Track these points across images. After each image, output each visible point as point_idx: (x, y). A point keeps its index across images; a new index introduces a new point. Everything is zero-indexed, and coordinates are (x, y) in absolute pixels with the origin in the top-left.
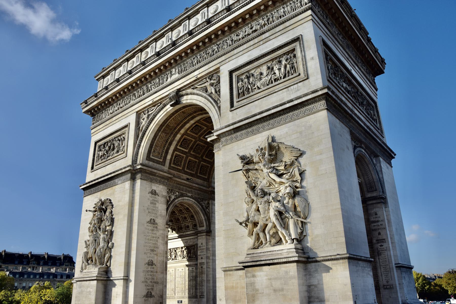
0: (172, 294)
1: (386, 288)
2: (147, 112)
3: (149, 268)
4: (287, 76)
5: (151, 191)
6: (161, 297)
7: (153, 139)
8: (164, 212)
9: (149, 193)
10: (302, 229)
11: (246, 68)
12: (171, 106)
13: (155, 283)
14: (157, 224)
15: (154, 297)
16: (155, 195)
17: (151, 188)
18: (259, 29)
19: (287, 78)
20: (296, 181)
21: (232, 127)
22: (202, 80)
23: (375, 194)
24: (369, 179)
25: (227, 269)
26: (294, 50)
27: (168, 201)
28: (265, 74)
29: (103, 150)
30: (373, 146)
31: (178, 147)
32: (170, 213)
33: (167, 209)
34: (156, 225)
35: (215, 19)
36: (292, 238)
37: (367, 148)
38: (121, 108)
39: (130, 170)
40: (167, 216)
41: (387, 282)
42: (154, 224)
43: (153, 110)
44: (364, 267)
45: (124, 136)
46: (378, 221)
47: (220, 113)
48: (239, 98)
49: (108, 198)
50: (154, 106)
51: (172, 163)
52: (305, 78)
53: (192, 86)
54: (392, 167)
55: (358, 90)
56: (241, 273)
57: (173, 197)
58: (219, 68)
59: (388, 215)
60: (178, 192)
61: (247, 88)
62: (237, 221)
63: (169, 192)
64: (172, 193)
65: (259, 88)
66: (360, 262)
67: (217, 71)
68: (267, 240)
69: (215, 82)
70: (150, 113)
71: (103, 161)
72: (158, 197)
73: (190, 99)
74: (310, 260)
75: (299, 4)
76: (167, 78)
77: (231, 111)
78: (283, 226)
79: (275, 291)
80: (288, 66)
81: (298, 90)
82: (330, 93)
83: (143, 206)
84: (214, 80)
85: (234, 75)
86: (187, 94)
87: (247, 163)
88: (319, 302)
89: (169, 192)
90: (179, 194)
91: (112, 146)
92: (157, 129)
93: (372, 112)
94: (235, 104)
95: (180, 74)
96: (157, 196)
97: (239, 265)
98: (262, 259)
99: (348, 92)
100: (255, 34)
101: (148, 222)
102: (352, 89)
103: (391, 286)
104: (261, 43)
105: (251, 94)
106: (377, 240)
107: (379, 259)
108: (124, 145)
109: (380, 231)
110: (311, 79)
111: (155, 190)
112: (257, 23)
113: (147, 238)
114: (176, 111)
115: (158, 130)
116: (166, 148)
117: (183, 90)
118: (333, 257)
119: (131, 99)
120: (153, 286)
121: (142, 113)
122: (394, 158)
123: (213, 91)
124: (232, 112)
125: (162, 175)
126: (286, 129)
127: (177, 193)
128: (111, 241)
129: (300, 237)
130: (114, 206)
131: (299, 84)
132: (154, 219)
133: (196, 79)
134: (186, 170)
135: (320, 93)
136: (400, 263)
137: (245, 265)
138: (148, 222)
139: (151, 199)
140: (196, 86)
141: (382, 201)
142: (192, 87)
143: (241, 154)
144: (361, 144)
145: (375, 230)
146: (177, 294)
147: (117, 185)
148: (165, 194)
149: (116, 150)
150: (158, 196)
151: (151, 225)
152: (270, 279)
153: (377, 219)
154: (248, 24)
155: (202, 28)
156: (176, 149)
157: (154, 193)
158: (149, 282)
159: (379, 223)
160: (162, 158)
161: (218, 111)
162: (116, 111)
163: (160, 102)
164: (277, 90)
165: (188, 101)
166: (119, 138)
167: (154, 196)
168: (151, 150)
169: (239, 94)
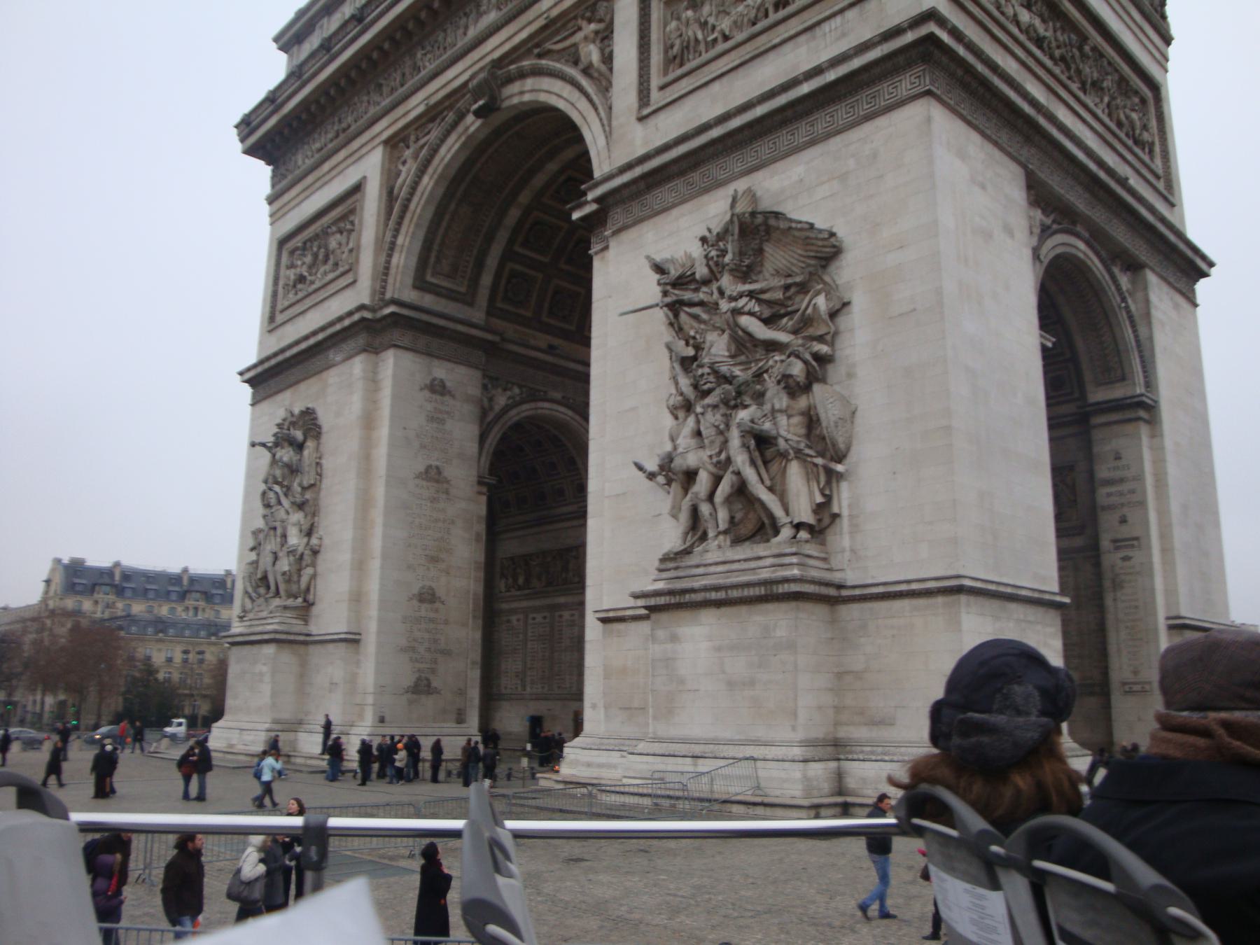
0: (517, 688)
1: (1131, 692)
5: (428, 382)
7: (432, 221)
8: (472, 447)
12: (478, 114)
14: (448, 482)
15: (439, 693)
16: (442, 394)
20: (820, 339)
21: (638, 171)
22: (564, 25)
23: (1117, 392)
25: (611, 614)
27: (484, 413)
29: (299, 263)
30: (1121, 234)
33: (482, 438)
34: (445, 485)
36: (796, 521)
37: (1097, 238)
38: (344, 130)
39: (363, 320)
40: (483, 459)
41: (1135, 673)
42: (437, 481)
43: (429, 132)
44: (1029, 622)
45: (351, 218)
46: (1121, 481)
47: (610, 125)
48: (666, 73)
49: (310, 406)
50: (432, 120)
53: (537, 45)
54: (1196, 305)
55: (1084, 38)
56: (644, 627)
57: (501, 400)
59: (1159, 462)
60: (520, 387)
61: (692, 38)
62: (640, 468)
63: (490, 386)
64: (500, 390)
65: (726, 38)
66: (1013, 606)
68: (718, 527)
69: (601, 26)
70: (422, 142)
71: (300, 295)
73: (532, 91)
74: (845, 593)
76: (466, 28)
77: (641, 119)
78: (768, 483)
79: (731, 684)
82: (944, 36)
84: (601, 21)
86: (522, 75)
88: (866, 724)
89: (490, 386)
90: (521, 394)
91: (322, 250)
92: (441, 191)
96: (447, 398)
97: (631, 602)
99: (1039, 41)
102: (1059, 34)
103: (1147, 687)
105: (706, 57)
106: (1115, 541)
107: (1115, 600)
108: (351, 245)
109: (1125, 510)
111: (442, 381)
114: (497, 133)
116: (475, 252)
118: (914, 586)
119: (369, 102)
120: (436, 663)
122: (1205, 275)
123: (595, 57)
124: (645, 121)
127: (516, 390)
132: (437, 468)
134: (545, 319)
135: (910, 37)
136: (1183, 613)
137: (652, 602)
138: (419, 476)
139: (429, 407)
140: (548, 46)
141: (1142, 413)
142: (536, 51)
143: (658, 258)
144: (1074, 223)
145: (1111, 508)
146: (528, 689)
148: (475, 391)
149: (331, 262)
150: (453, 396)
151: (429, 484)
152: (719, 649)
153: (1117, 474)
156: (508, 255)
157: (437, 388)
159: (1125, 487)
161: (605, 122)
162: (331, 140)
166: (342, 225)
167: (438, 397)
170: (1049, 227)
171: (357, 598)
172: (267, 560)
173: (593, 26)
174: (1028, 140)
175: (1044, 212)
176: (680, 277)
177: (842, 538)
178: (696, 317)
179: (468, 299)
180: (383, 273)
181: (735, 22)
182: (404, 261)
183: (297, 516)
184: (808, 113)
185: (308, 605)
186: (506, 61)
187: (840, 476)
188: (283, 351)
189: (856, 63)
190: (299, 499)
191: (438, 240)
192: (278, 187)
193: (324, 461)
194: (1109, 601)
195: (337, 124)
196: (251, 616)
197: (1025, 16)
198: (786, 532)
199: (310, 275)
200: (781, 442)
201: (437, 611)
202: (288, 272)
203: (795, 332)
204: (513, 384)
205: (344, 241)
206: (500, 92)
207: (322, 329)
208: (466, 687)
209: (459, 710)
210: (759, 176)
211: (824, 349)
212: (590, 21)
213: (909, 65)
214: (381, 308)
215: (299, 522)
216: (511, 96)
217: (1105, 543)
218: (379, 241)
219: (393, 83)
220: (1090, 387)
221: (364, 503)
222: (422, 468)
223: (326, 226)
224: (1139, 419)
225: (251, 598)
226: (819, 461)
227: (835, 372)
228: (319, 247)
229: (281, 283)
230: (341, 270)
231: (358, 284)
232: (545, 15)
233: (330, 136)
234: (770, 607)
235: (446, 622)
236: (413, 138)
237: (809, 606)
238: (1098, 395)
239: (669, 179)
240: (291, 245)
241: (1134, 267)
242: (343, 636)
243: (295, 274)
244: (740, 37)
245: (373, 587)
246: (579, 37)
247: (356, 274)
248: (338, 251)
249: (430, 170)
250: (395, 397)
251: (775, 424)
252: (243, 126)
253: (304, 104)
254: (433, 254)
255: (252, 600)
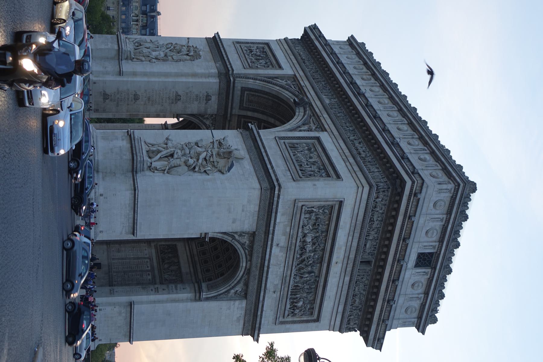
1: (111, 290)
2: (294, 83)
3: (132, 96)
4: (302, 172)
5: (209, 94)
6: (104, 111)
9: (207, 92)
10: (160, 169)
11: (320, 149)
13: (118, 103)
14: (176, 103)
17: (213, 95)
18: (360, 156)
19: (300, 172)
24: (220, 284)
26: (328, 176)
27: (202, 116)
28: (310, 160)
29: (258, 51)
31: (263, 124)
32: (189, 119)
34: (175, 102)
35: (378, 122)
37: (248, 272)
39: (229, 71)
43: (295, 88)
45: (271, 66)
46: (176, 289)
48: (288, 143)
49: (202, 57)
50: (299, 89)
51: (245, 119)
52: (295, 179)
58: (326, 131)
59: (182, 301)
63: (212, 118)
64: (211, 122)
66: (132, 213)
67: (323, 129)
72: (204, 103)
74: (135, 173)
75: (378, 180)
77: (275, 138)
78: (162, 157)
79: (112, 149)
80: (313, 173)
81: (284, 176)
82: (276, 192)
83: (192, 87)
85: (316, 141)
86: (305, 111)
87: (220, 142)
89: (212, 118)
92: (274, 93)
93: (300, 304)
94: (283, 141)
95: (328, 104)
98: (136, 142)
100: (355, 152)
101: (176, 92)
104: (344, 157)
106: (157, 288)
110: (294, 184)
112: (368, 155)
113: (161, 93)
115: (274, 95)
116: (258, 108)
117: (311, 109)
121: (293, 80)
123: (302, 128)
125: (228, 107)
126: (248, 167)
128: (157, 61)
129: (153, 169)
130: (193, 62)
131: (291, 177)
132: (180, 99)
133: (319, 115)
135: (276, 183)
136: (135, 306)
138: (176, 92)
139: (201, 95)
141: (198, 295)
147: (215, 63)
148: (209, 111)
150: (206, 104)
154: (370, 149)
155: (371, 113)
157: (208, 98)
158: (118, 96)
159: (174, 290)
160: (247, 106)
162: (301, 58)
163: (303, 92)
164: (288, 163)
165: (297, 114)
166: (269, 63)
167: (205, 98)
168: (253, 92)
169: (293, 144)
170: (245, 248)
171: (134, 74)
172: (147, 45)
173: (314, 128)
174: (265, 233)
175: (249, 246)
176: (222, 143)
177: (148, 173)
178: (210, 147)
179: (241, 108)
180: (246, 77)
181: (299, 157)
182: (251, 83)
183: (162, 54)
184: (264, 169)
185: (132, 59)
186: (311, 107)
187: (164, 173)
188: (223, 47)
189: (273, 175)
190: (168, 54)
191: (259, 94)
192: (290, 42)
193: (182, 62)
194: (138, 287)
195: (308, 59)
196: (127, 41)
197: (309, 239)
198: (149, 160)
199: (252, 55)
200: (172, 159)
201: (132, 101)
202: (256, 47)
203: (202, 164)
204: (215, 127)
205: (262, 65)
206: (301, 106)
207: (228, 59)
208: (106, 112)
209: (98, 110)
210: (249, 160)
211: (197, 169)
212: (316, 128)
213: (270, 185)
214: (233, 76)
215: (160, 55)
216: (299, 110)
217: (156, 286)
218: (258, 75)
219: (316, 76)
220: (207, 283)
221: (167, 75)
222: (179, 94)
223: (270, 58)
224: (195, 293)
225: (134, 41)
226: (168, 168)
227: (191, 173)
228: (262, 57)
229: (250, 45)
230: (250, 64)
231: (244, 69)
232: (321, 115)
233: (304, 58)
234: (131, 155)
235: (128, 104)
236: (294, 83)
237: (131, 164)
238: (204, 285)
239: (254, 144)
240: (266, 47)
241: (245, 295)
242: (121, 70)
243: (253, 49)
244: (293, 157)
245: (138, 79)
246: (312, 124)
247: (247, 68)
248: (258, 63)
249: (281, 89)
250: (202, 83)
251: (177, 158)
252: (314, 26)
253: (316, 48)
254: (254, 93)
255: (133, 41)
